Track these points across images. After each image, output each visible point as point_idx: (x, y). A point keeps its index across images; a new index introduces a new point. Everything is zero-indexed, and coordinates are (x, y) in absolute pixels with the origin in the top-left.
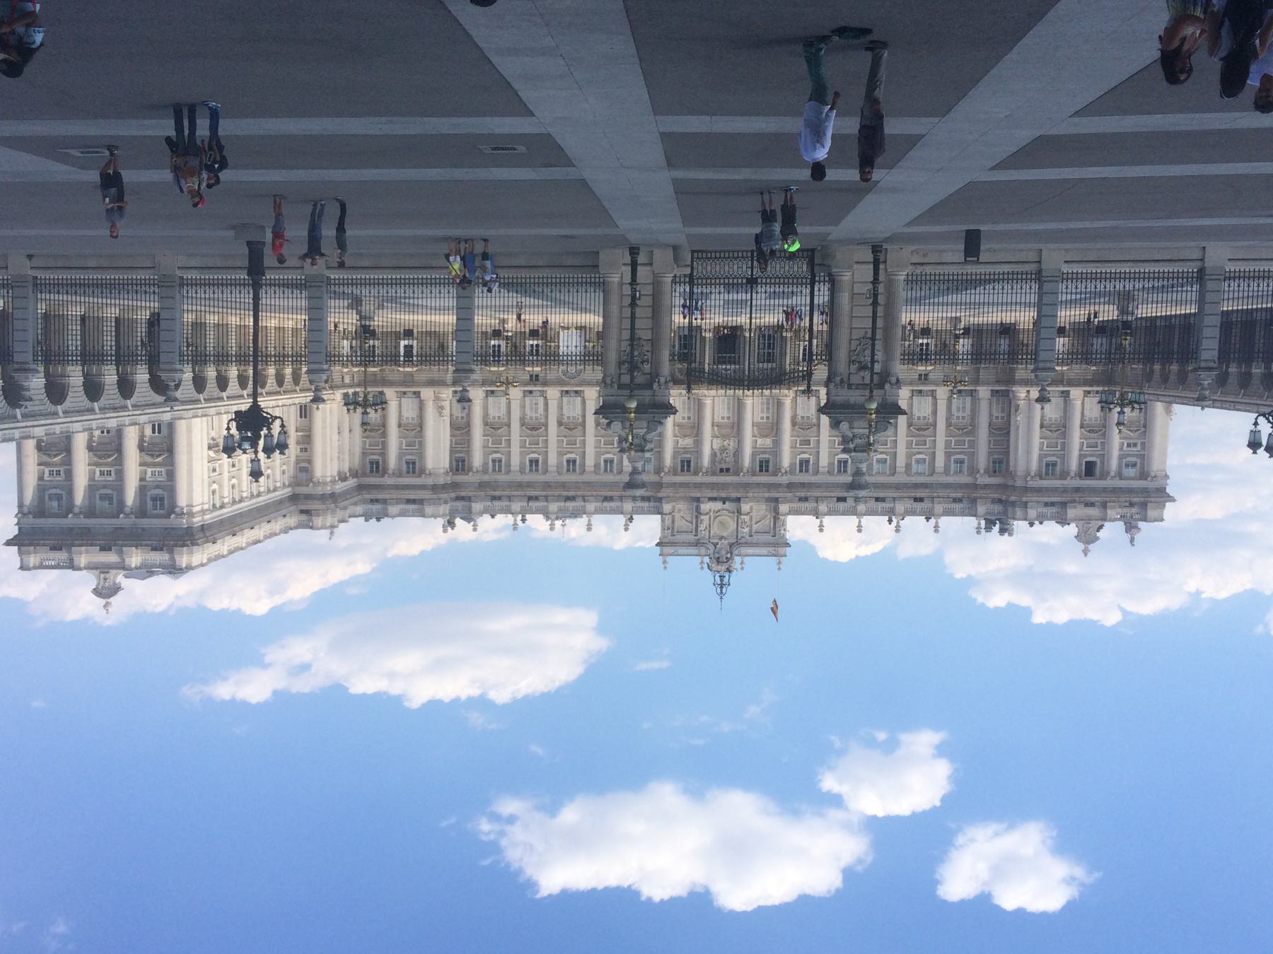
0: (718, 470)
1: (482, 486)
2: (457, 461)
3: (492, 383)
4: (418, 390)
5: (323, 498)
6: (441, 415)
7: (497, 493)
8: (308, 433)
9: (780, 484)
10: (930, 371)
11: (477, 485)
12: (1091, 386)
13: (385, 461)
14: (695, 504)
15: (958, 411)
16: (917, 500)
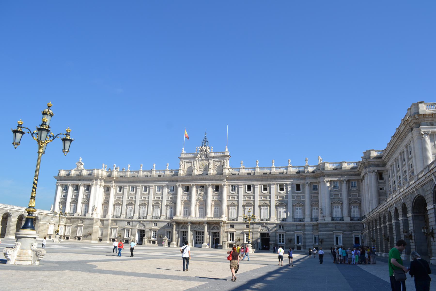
0: (204, 186)
1: (304, 178)
2: (317, 189)
3: (300, 225)
4: (332, 221)
5: (370, 165)
6: (322, 210)
7: (297, 175)
8: (380, 197)
9: (180, 181)
10: (126, 226)
11: (306, 178)
12: (72, 218)
13: (349, 187)
14: (213, 173)
15: (118, 210)
16: (135, 176)
